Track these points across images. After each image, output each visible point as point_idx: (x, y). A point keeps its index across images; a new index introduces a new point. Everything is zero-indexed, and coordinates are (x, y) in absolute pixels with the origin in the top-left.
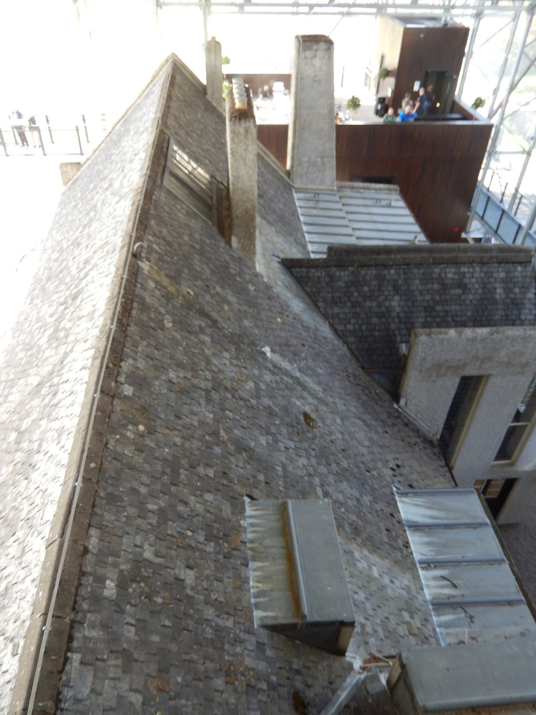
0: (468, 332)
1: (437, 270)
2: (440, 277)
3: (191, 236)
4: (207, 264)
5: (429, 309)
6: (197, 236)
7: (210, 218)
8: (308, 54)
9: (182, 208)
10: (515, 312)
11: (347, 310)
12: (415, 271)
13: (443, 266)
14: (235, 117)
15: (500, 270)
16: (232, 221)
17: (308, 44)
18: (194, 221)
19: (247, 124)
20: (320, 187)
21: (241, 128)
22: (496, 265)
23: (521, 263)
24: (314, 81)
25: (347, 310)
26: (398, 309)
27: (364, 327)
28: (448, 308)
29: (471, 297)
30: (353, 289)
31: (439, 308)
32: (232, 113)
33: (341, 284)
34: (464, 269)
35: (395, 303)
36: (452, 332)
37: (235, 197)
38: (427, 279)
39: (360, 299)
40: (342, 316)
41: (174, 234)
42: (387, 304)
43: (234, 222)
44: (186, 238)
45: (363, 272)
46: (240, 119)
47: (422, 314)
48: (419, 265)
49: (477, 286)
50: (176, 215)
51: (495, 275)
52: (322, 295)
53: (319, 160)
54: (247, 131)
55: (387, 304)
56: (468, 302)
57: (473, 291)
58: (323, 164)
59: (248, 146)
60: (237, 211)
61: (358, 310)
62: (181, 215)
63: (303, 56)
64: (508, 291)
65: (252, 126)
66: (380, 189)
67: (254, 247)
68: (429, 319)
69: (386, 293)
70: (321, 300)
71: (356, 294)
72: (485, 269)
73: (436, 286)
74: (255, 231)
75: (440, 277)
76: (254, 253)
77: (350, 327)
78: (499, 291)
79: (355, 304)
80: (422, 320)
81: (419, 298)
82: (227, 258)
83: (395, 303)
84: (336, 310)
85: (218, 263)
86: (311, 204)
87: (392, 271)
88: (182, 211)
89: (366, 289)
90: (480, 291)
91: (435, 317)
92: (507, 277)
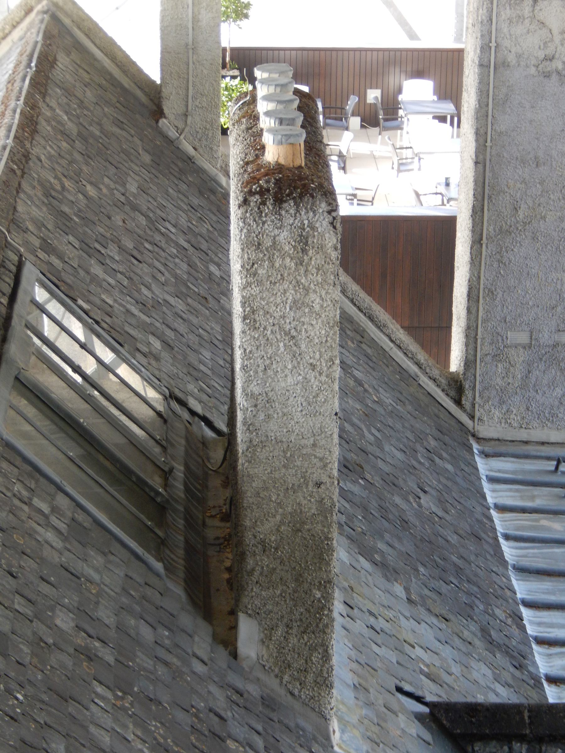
3: (81, 612)
4: (141, 724)
6: (106, 614)
7: (160, 546)
9: (54, 509)
14: (262, 192)
16: (241, 557)
18: (98, 560)
19: (305, 217)
21: (282, 230)
24: (547, 75)
32: (254, 180)
37: (255, 471)
41: (19, 604)
43: (250, 562)
44: (64, 621)
46: (279, 201)
50: (30, 534)
54: (303, 242)
59: (307, 290)
60: (263, 522)
62: (50, 536)
65: (322, 223)
67: (326, 657)
74: (328, 598)
76: (324, 682)
82: (220, 699)
85: (180, 716)
86: (542, 498)
88: (54, 520)
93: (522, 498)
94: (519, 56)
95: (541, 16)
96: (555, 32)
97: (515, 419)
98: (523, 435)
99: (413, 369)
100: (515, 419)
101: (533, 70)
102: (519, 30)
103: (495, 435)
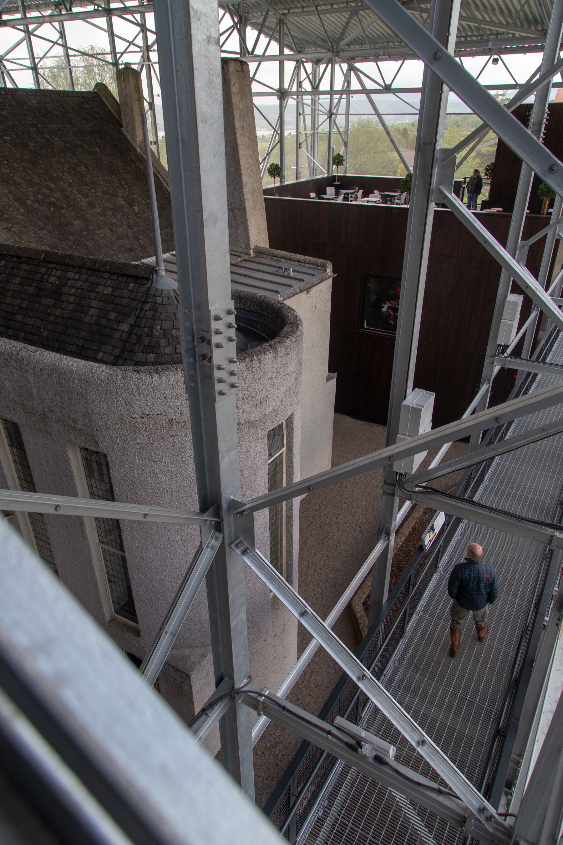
2: (41, 281)
13: (52, 266)
29: (58, 312)
34: (71, 275)
49: (72, 299)
56: (52, 318)
57: (65, 305)
66: (305, 262)
72: (93, 279)
73: (31, 290)
75: (41, 281)
78: (92, 312)
90: (71, 307)
91: (9, 328)
92: (112, 295)
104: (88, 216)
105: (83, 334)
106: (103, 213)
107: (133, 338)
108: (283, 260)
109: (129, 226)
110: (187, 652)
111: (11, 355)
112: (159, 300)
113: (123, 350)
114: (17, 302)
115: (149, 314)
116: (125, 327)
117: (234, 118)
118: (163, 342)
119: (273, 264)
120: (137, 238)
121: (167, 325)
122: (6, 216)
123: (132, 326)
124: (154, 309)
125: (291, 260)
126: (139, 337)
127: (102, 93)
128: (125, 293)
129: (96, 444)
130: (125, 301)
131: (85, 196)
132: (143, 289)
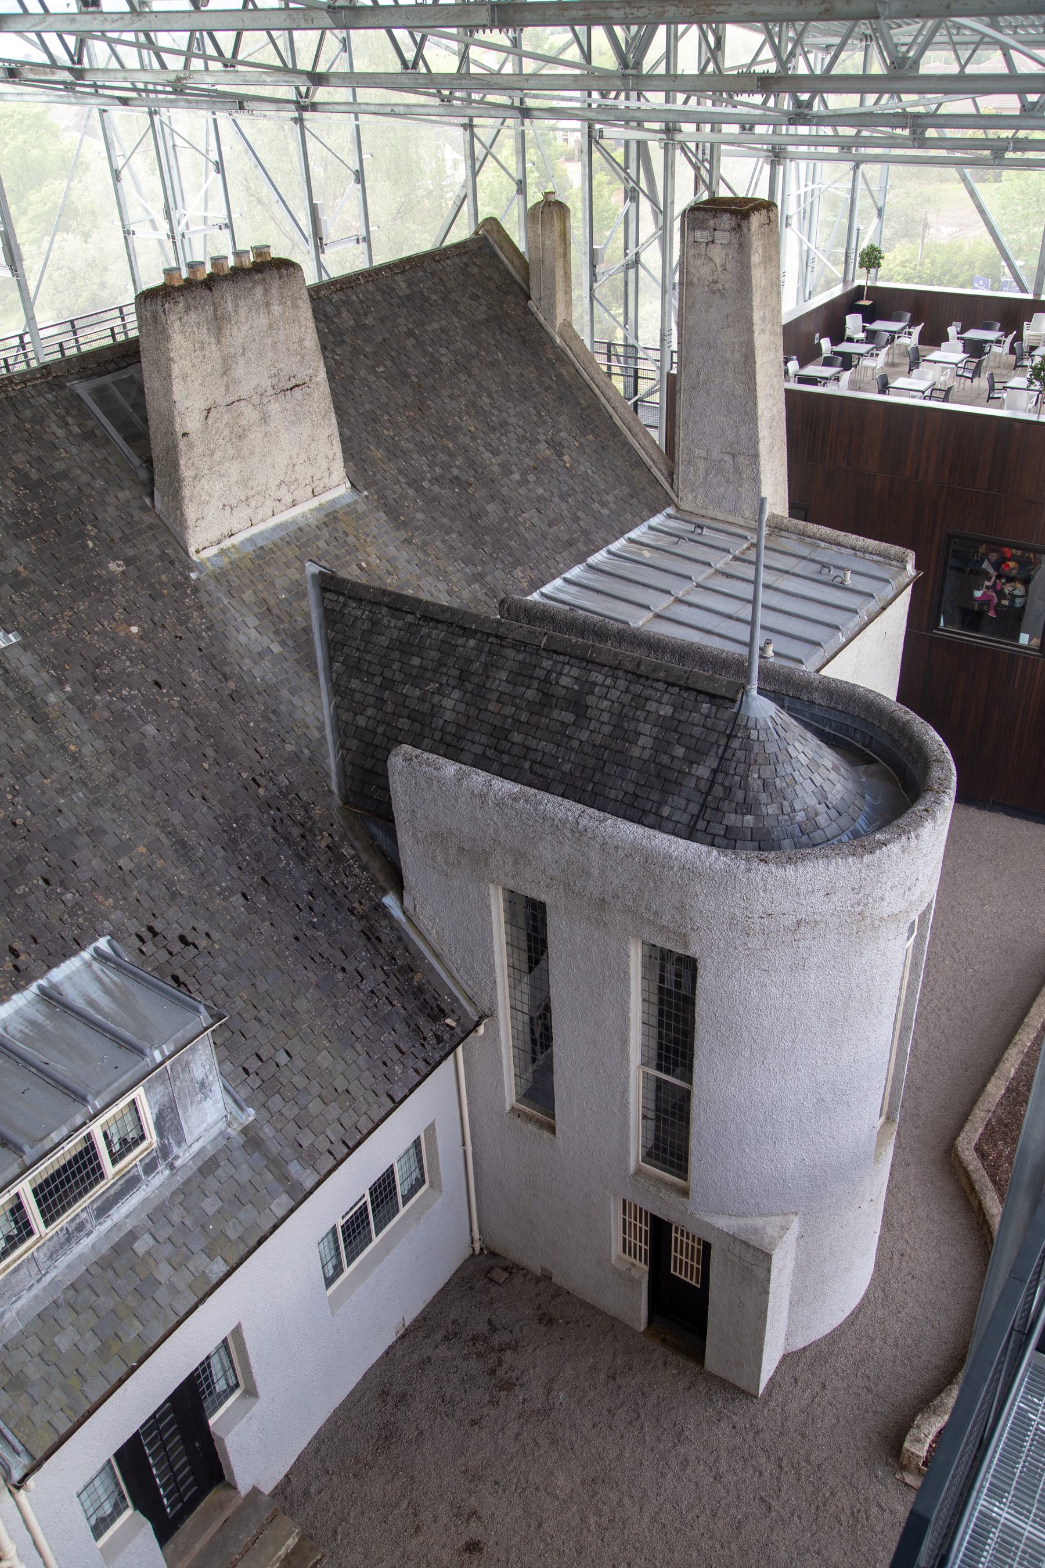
0: (479, 778)
1: (547, 664)
2: (546, 681)
5: (499, 733)
8: (700, 235)
10: (655, 796)
11: (370, 689)
12: (511, 653)
13: (561, 658)
15: (666, 698)
17: (700, 215)
20: (731, 519)
22: (661, 686)
23: (712, 697)
24: (714, 293)
25: (370, 689)
26: (448, 716)
27: (380, 730)
28: (533, 743)
29: (584, 735)
30: (396, 655)
31: (517, 737)
33: (383, 640)
34: (596, 677)
35: (448, 703)
36: (451, 768)
38: (522, 675)
39: (398, 677)
40: (358, 697)
42: (436, 699)
45: (425, 630)
47: (484, 739)
48: (517, 645)
49: (605, 717)
51: (651, 706)
52: (346, 650)
53: (728, 459)
55: (436, 699)
56: (575, 744)
57: (593, 725)
58: (737, 470)
61: (386, 695)
63: (691, 239)
64: (661, 745)
66: (864, 551)
68: (490, 753)
69: (444, 680)
70: (342, 659)
71: (396, 666)
72: (637, 688)
73: (531, 694)
75: (546, 681)
77: (361, 721)
78: (642, 741)
79: (388, 684)
80: (478, 749)
81: (492, 706)
83: (448, 703)
84: (355, 684)
87: (472, 643)
89: (416, 661)
90: (606, 729)
91: (503, 752)
92: (672, 718)
93: (653, 540)
94: (699, 279)
95: (710, 254)
96: (718, 265)
97: (700, 502)
98: (703, 512)
99: (649, 462)
100: (700, 502)
101: (706, 288)
102: (699, 262)
103: (689, 509)
104: (504, 491)
105: (633, 775)
106: (524, 482)
107: (718, 791)
108: (822, 544)
109: (563, 497)
110: (760, 1222)
111: (564, 822)
112: (754, 734)
113: (704, 806)
114: (509, 710)
115: (740, 754)
116: (703, 771)
117: (752, 306)
118: (763, 797)
119: (805, 552)
120: (576, 519)
121: (767, 772)
122: (402, 518)
123: (715, 772)
124: (747, 748)
125: (839, 544)
126: (728, 790)
127: (493, 238)
128: (695, 717)
129: (686, 945)
130: (697, 731)
131: (495, 453)
132: (726, 715)
